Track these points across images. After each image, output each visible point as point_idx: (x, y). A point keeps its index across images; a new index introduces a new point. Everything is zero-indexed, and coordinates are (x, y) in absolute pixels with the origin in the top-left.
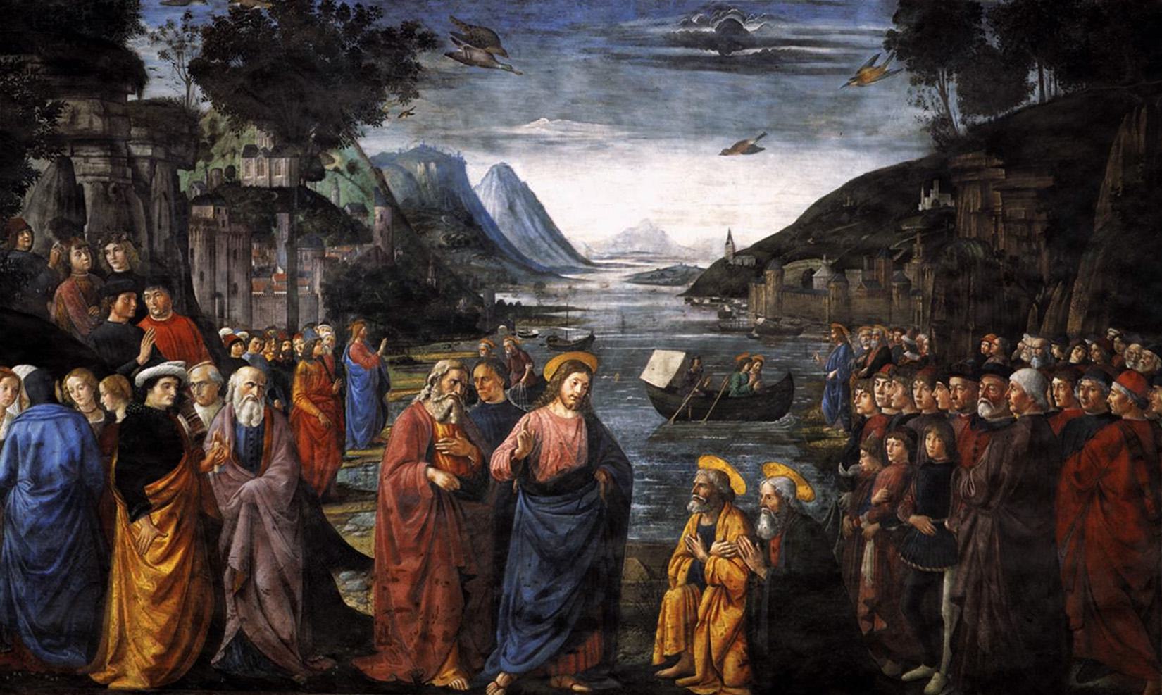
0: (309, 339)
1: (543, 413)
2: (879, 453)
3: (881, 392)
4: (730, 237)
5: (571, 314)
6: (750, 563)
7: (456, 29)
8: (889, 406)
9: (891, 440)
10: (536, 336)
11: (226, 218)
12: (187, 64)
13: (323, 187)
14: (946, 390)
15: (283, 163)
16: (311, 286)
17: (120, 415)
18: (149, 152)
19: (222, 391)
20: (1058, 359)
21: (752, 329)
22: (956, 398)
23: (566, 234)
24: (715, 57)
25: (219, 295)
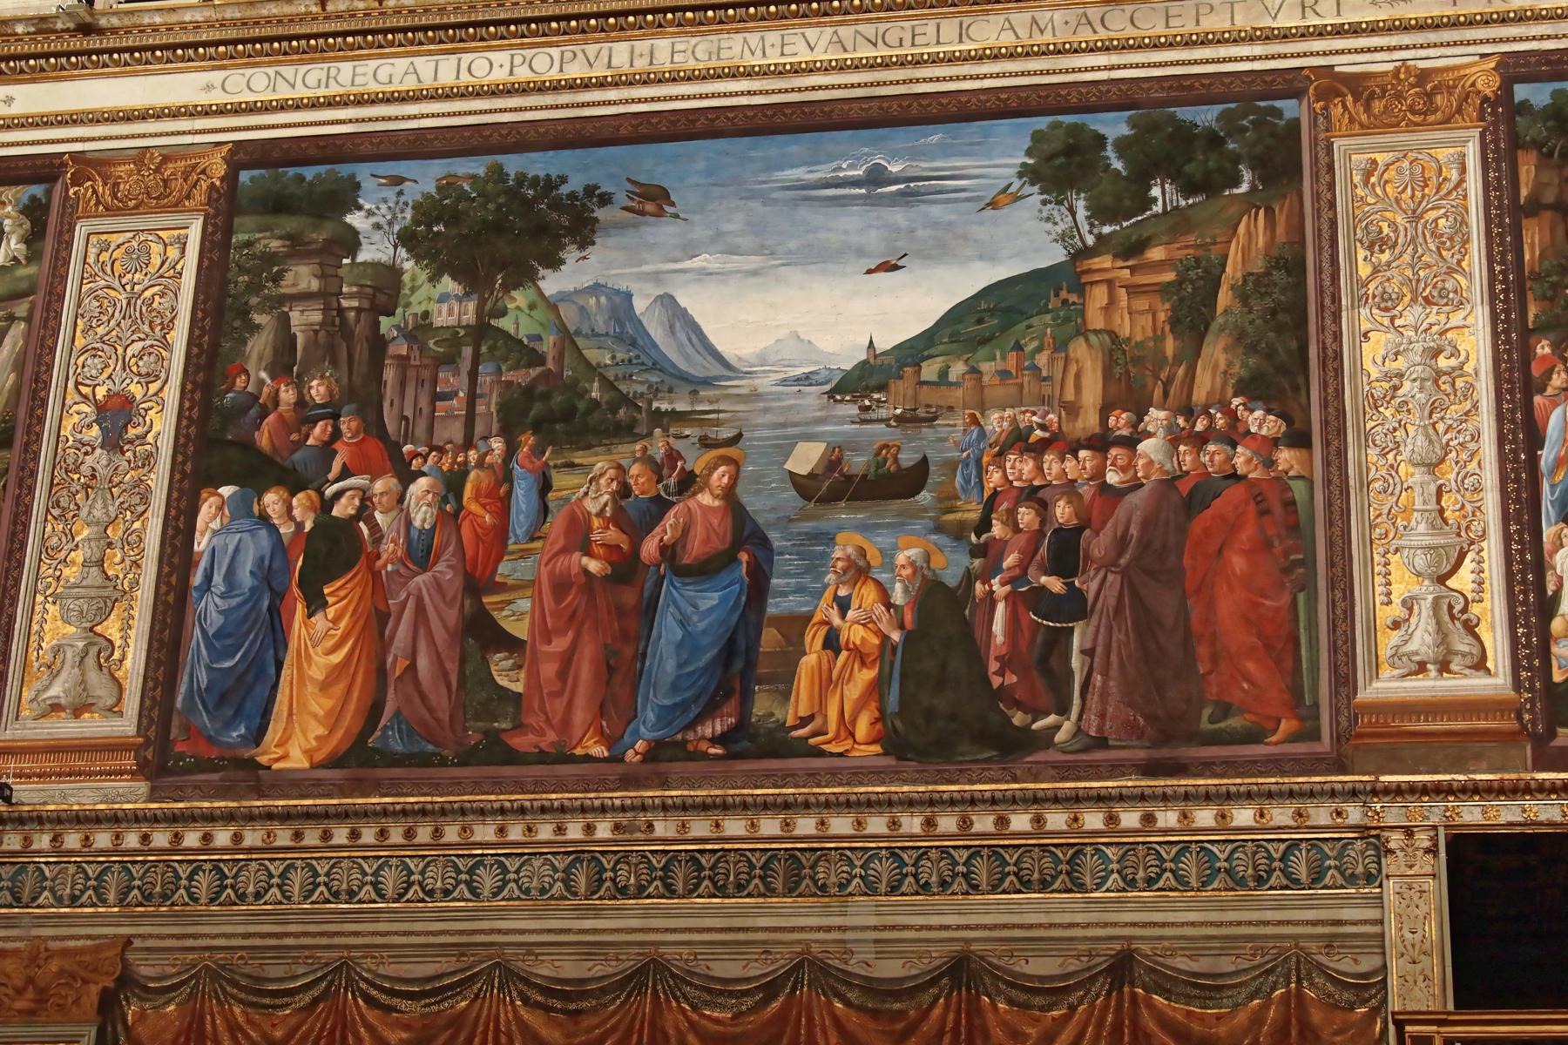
0: (483, 450)
1: (692, 503)
2: (1012, 521)
3: (1013, 467)
4: (871, 342)
5: (721, 415)
6: (884, 627)
7: (630, 187)
8: (1020, 479)
9: (1023, 510)
10: (687, 436)
11: (417, 353)
12: (395, 231)
13: (505, 323)
14: (1075, 462)
15: (471, 306)
16: (488, 405)
17: (308, 526)
18: (355, 304)
19: (401, 499)
20: (1183, 429)
21: (889, 419)
22: (1085, 469)
23: (719, 348)
24: (862, 195)
25: (406, 419)
